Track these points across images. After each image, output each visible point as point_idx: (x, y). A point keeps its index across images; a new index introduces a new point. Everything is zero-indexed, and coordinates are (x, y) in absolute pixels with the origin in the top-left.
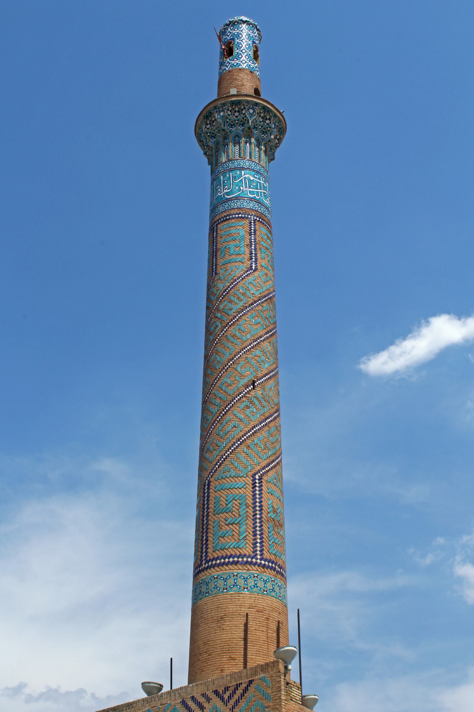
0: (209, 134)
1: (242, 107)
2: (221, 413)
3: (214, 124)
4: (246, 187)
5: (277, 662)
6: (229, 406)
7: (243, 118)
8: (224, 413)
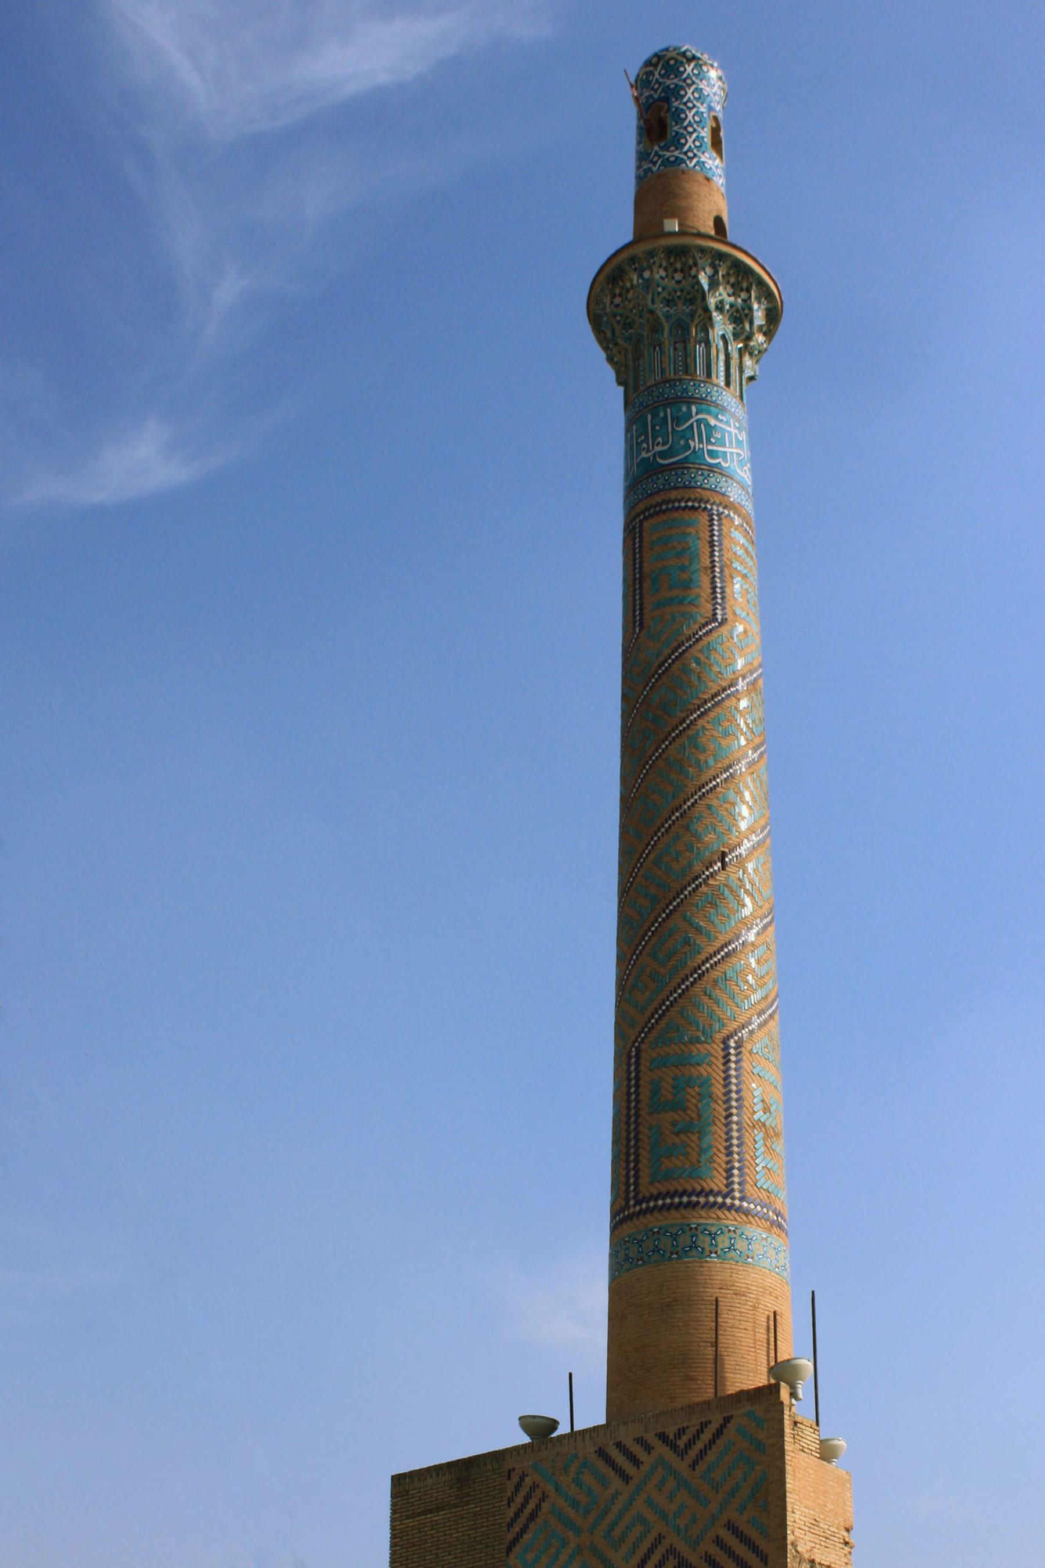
0: (618, 318)
1: (691, 262)
2: (660, 916)
3: (630, 295)
4: (701, 441)
5: (777, 1387)
6: (675, 903)
7: (693, 287)
8: (664, 915)
